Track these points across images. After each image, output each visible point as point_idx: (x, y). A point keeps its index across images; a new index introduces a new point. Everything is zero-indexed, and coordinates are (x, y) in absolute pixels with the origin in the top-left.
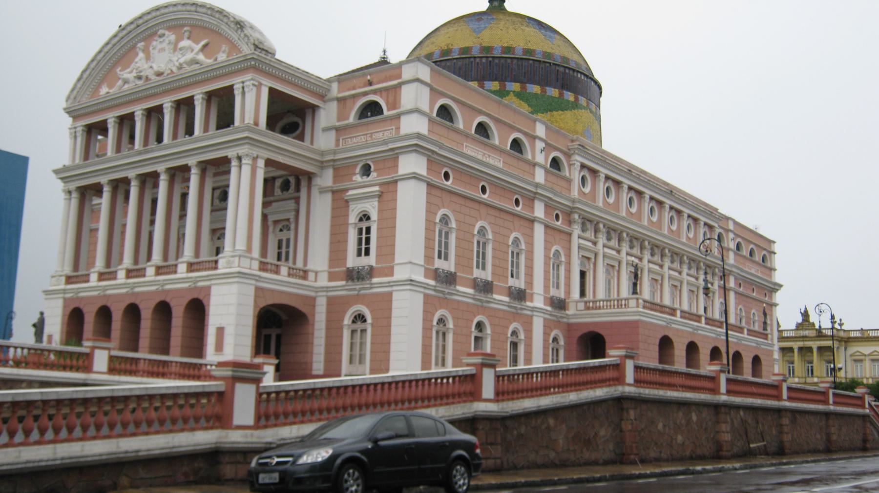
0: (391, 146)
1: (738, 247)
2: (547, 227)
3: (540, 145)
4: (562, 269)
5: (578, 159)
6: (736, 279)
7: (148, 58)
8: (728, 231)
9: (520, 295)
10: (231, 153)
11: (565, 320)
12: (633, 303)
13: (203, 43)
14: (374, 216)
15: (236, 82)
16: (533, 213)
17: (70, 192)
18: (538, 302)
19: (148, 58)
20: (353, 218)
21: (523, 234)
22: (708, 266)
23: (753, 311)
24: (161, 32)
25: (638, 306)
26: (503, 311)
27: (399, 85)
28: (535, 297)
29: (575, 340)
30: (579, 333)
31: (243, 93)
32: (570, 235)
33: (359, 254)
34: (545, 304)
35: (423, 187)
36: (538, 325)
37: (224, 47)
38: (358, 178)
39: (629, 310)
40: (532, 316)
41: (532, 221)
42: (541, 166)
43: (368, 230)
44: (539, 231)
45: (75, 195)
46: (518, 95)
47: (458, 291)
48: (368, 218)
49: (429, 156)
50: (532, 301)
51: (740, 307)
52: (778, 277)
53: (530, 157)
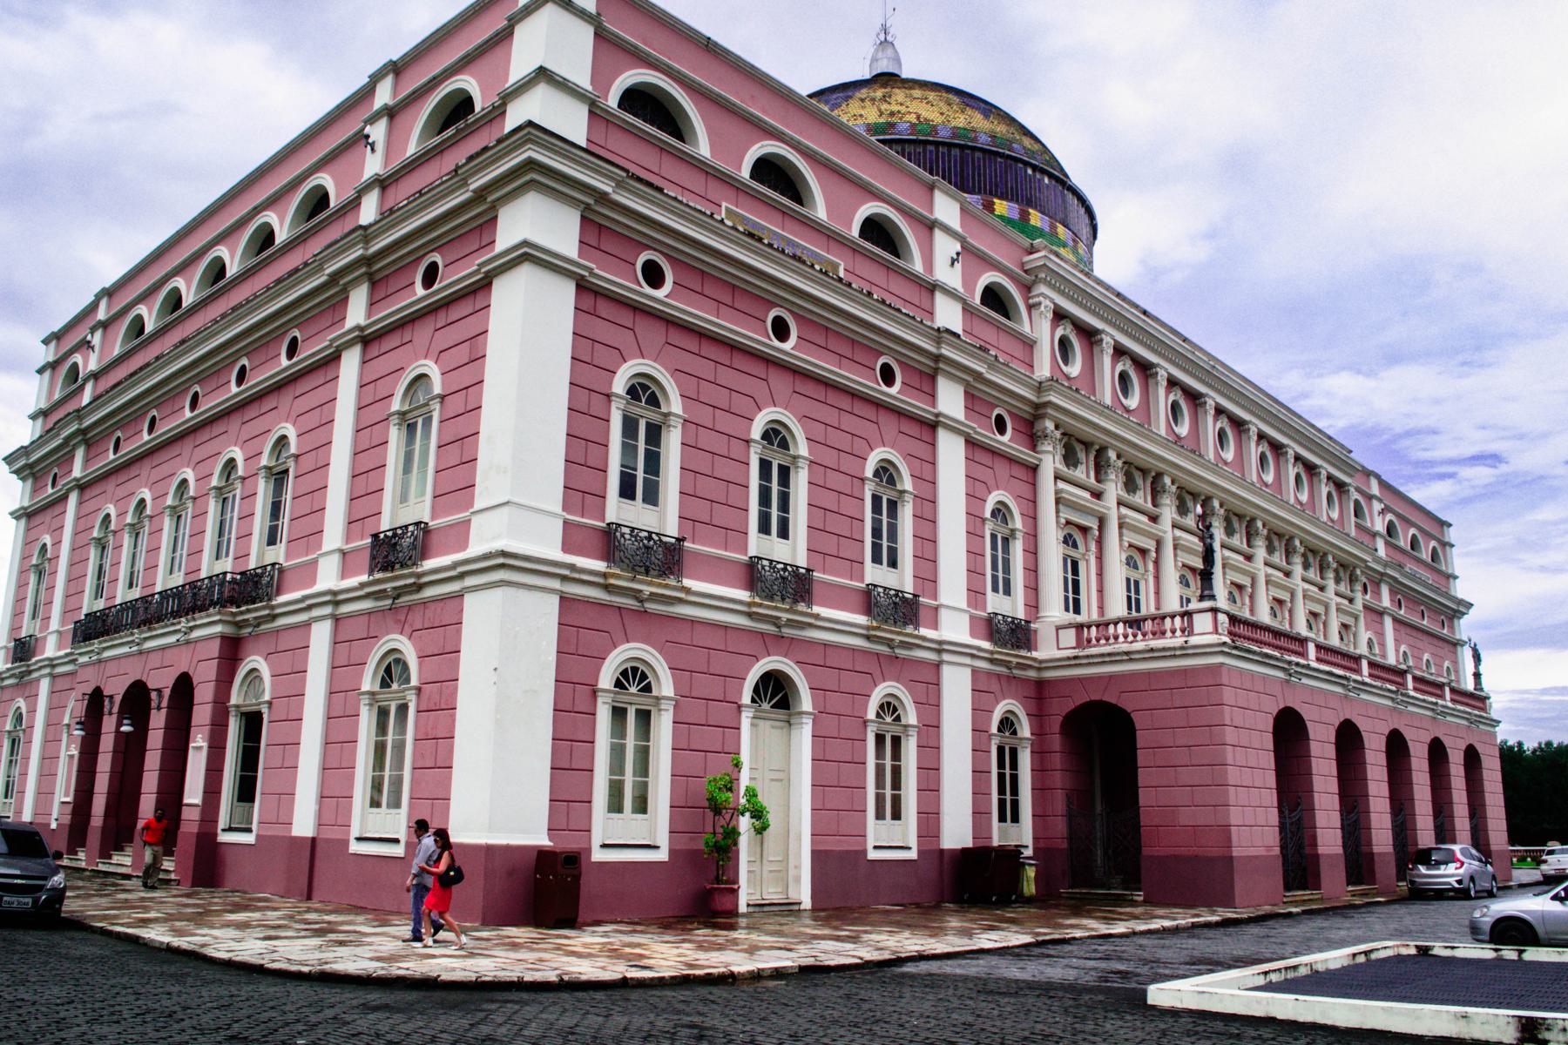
0: (476, 183)
1: (1391, 530)
2: (971, 443)
3: (945, 247)
4: (1018, 548)
5: (1047, 296)
6: (1393, 592)
8: (1370, 498)
9: (906, 609)
11: (1032, 674)
12: (1203, 622)
16: (934, 404)
18: (955, 627)
21: (909, 456)
22: (1342, 565)
23: (1426, 656)
25: (1216, 631)
26: (854, 650)
28: (943, 613)
29: (1055, 723)
30: (1070, 705)
32: (1034, 469)
34: (973, 635)
35: (568, 290)
36: (957, 687)
39: (1194, 640)
40: (937, 666)
41: (931, 426)
42: (950, 293)
44: (951, 453)
47: (688, 591)
49: (588, 207)
50: (935, 625)
51: (1403, 648)
52: (1461, 590)
53: (918, 266)
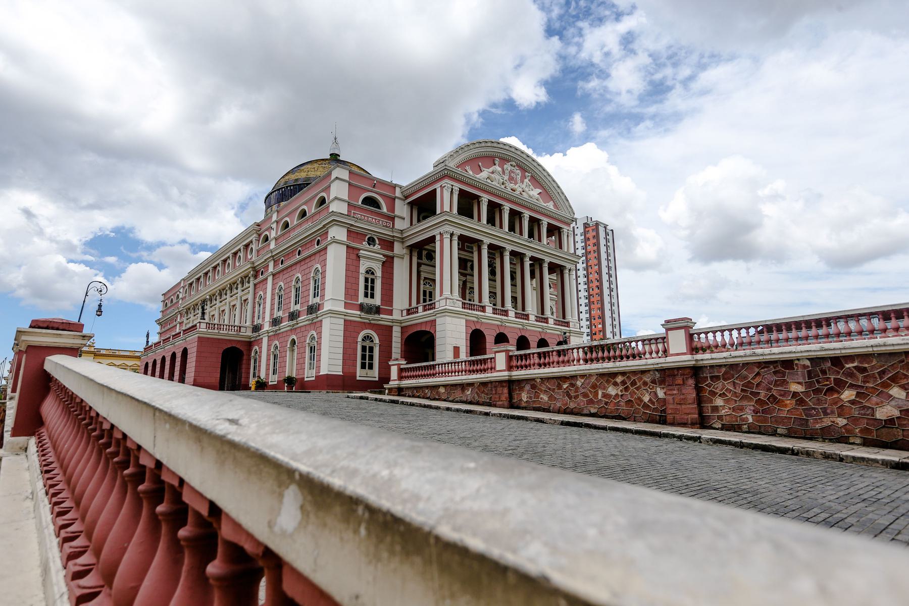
7: (504, 172)
10: (568, 266)
17: (452, 235)
19: (504, 172)
24: (514, 163)
45: (455, 238)
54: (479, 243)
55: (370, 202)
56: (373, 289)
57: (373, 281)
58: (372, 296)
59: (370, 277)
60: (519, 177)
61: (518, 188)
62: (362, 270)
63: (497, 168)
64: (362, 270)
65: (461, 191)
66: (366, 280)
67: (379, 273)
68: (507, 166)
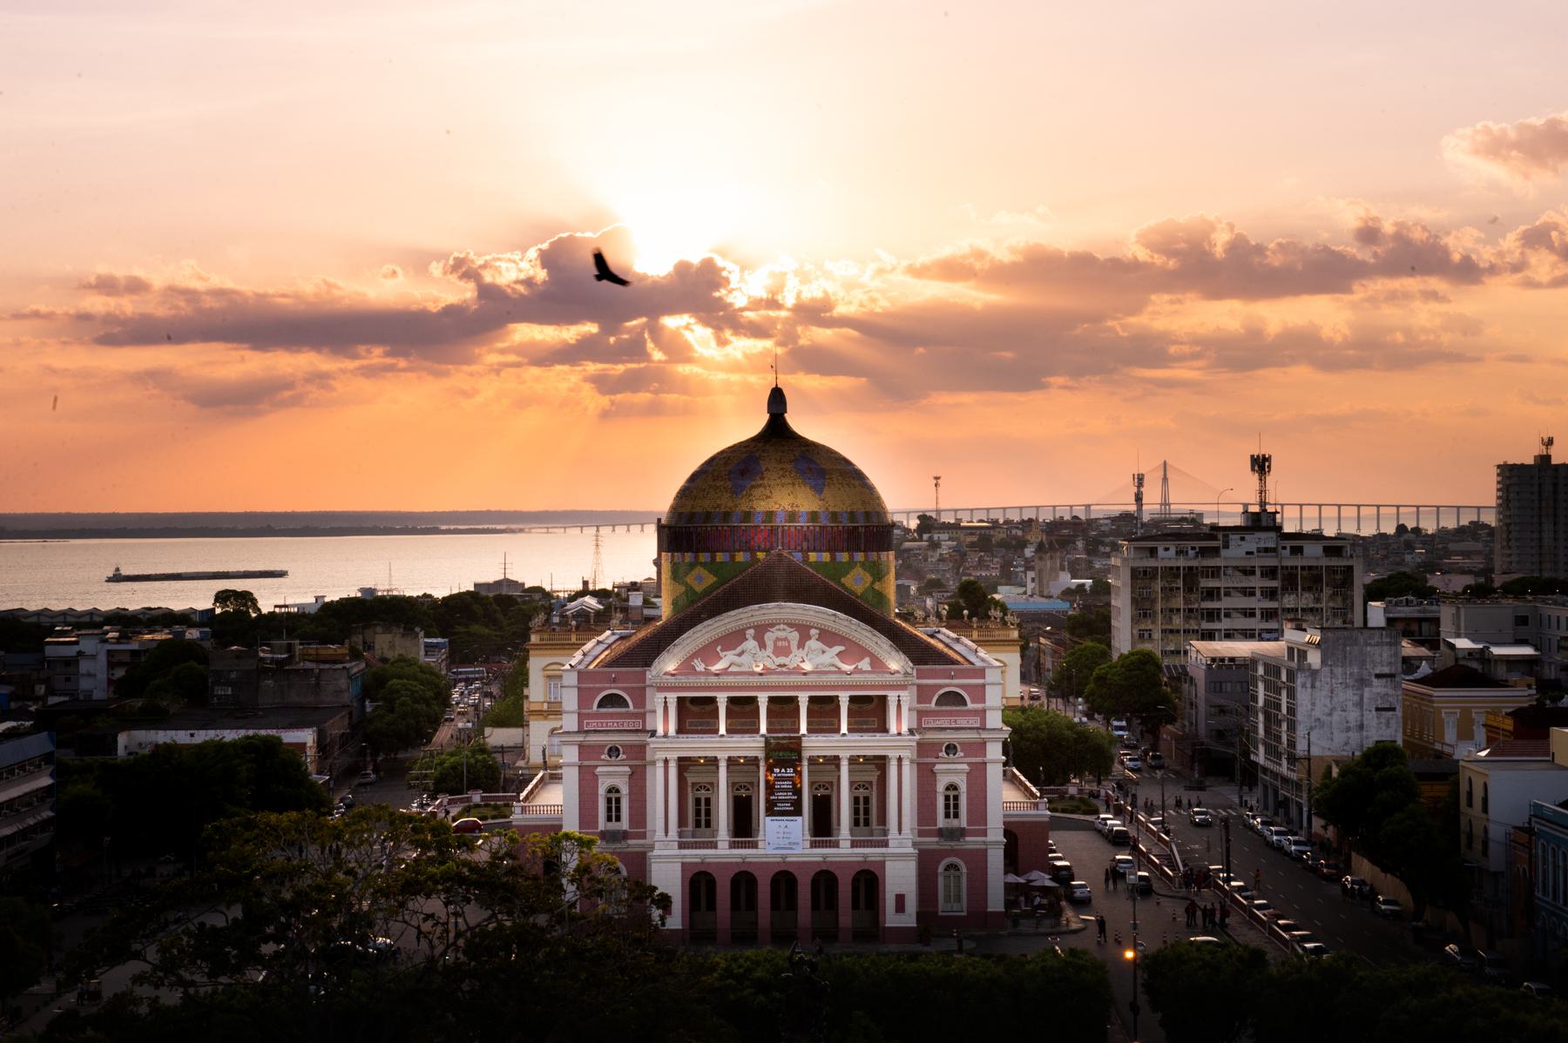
7: (762, 646)
10: (893, 754)
13: (842, 648)
14: (963, 788)
15: (892, 696)
17: (666, 761)
19: (762, 646)
20: (941, 788)
27: (984, 686)
31: (899, 706)
33: (947, 815)
37: (867, 660)
38: (943, 754)
43: (956, 798)
46: (863, 565)
48: (955, 788)
54: (714, 761)
55: (612, 701)
56: (618, 809)
57: (618, 800)
58: (618, 819)
59: (613, 796)
60: (794, 644)
61: (792, 661)
62: (602, 791)
63: (750, 644)
64: (602, 791)
65: (679, 699)
66: (609, 801)
67: (625, 790)
68: (769, 638)
